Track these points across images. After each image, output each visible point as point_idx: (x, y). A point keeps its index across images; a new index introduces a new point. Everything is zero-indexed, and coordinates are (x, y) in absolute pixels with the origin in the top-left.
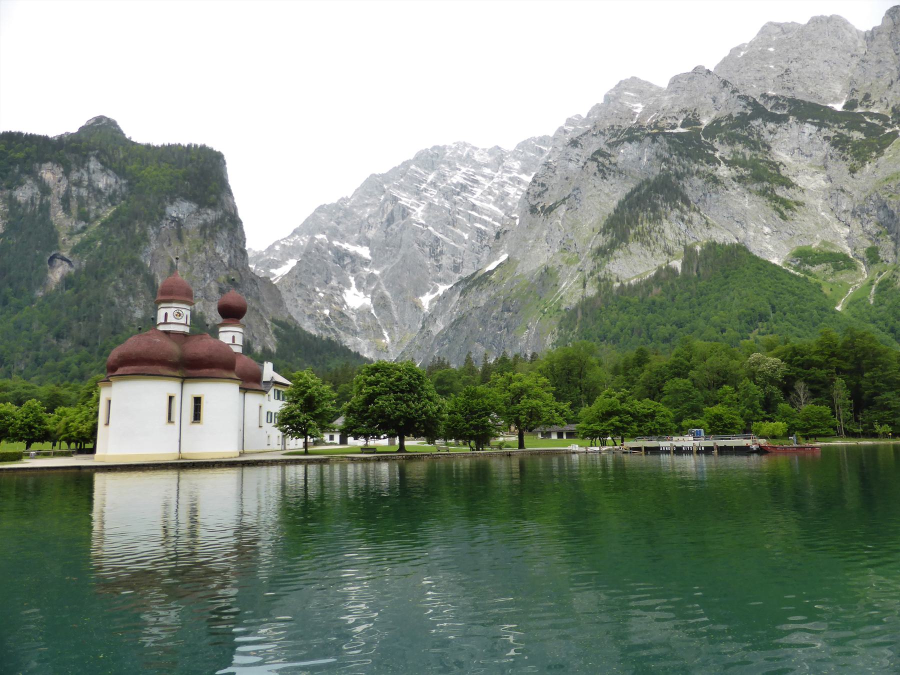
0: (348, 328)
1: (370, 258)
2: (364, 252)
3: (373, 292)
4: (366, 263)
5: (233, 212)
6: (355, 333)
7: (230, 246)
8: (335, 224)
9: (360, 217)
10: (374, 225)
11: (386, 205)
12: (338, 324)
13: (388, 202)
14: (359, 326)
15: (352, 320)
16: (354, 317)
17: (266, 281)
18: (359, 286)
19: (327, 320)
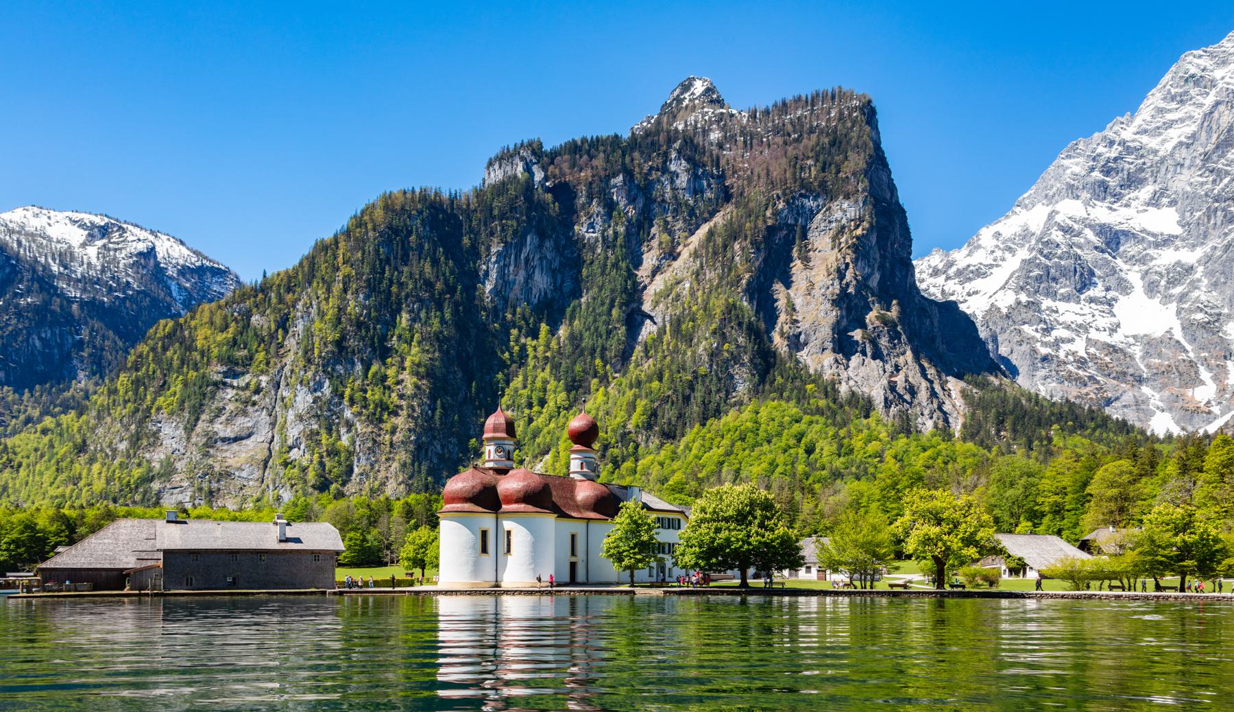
0: (1124, 374)
1: (1178, 231)
2: (1165, 221)
3: (1182, 298)
4: (1166, 241)
5: (888, 196)
6: (1140, 380)
7: (883, 257)
8: (1100, 176)
9: (1155, 152)
10: (1187, 163)
11: (1216, 115)
12: (1103, 368)
13: (1222, 108)
14: (1148, 366)
15: (1132, 357)
16: (1137, 351)
17: (950, 308)
18: (1151, 289)
19: (1081, 363)
